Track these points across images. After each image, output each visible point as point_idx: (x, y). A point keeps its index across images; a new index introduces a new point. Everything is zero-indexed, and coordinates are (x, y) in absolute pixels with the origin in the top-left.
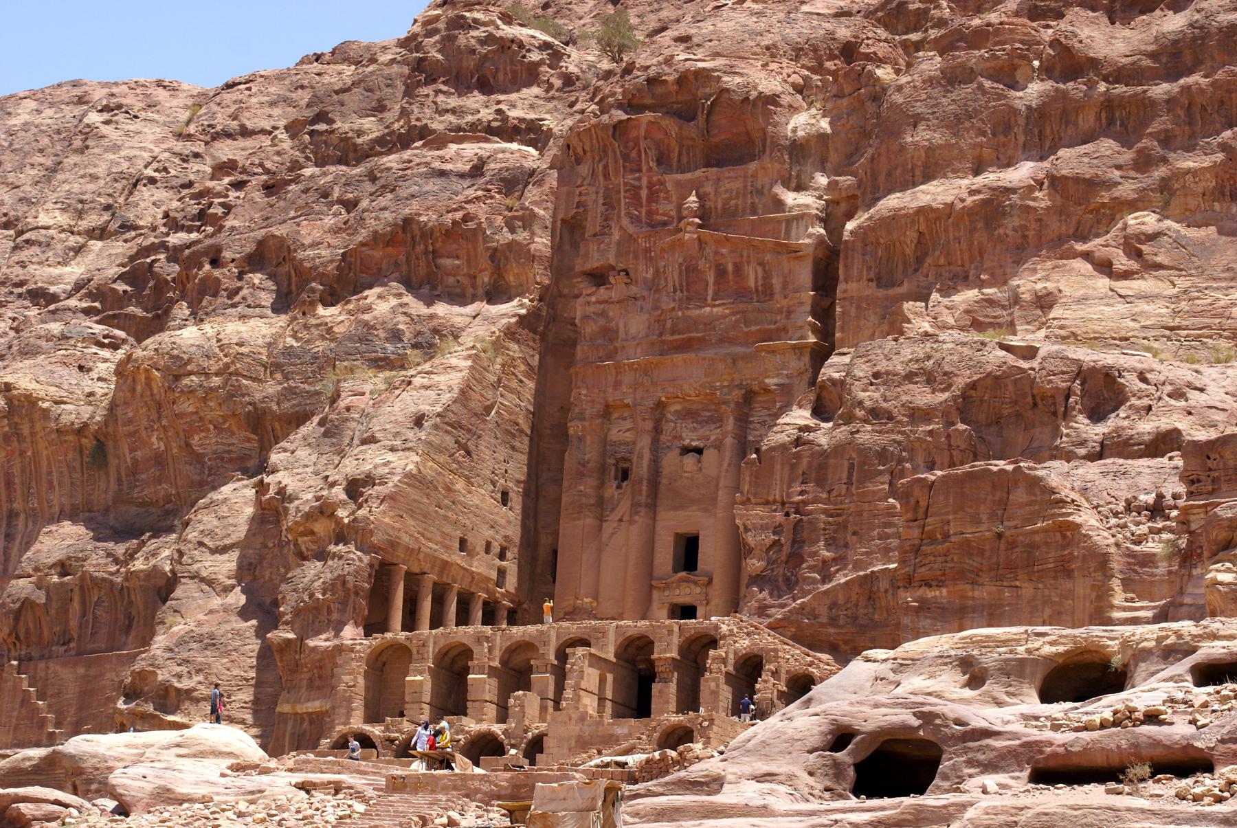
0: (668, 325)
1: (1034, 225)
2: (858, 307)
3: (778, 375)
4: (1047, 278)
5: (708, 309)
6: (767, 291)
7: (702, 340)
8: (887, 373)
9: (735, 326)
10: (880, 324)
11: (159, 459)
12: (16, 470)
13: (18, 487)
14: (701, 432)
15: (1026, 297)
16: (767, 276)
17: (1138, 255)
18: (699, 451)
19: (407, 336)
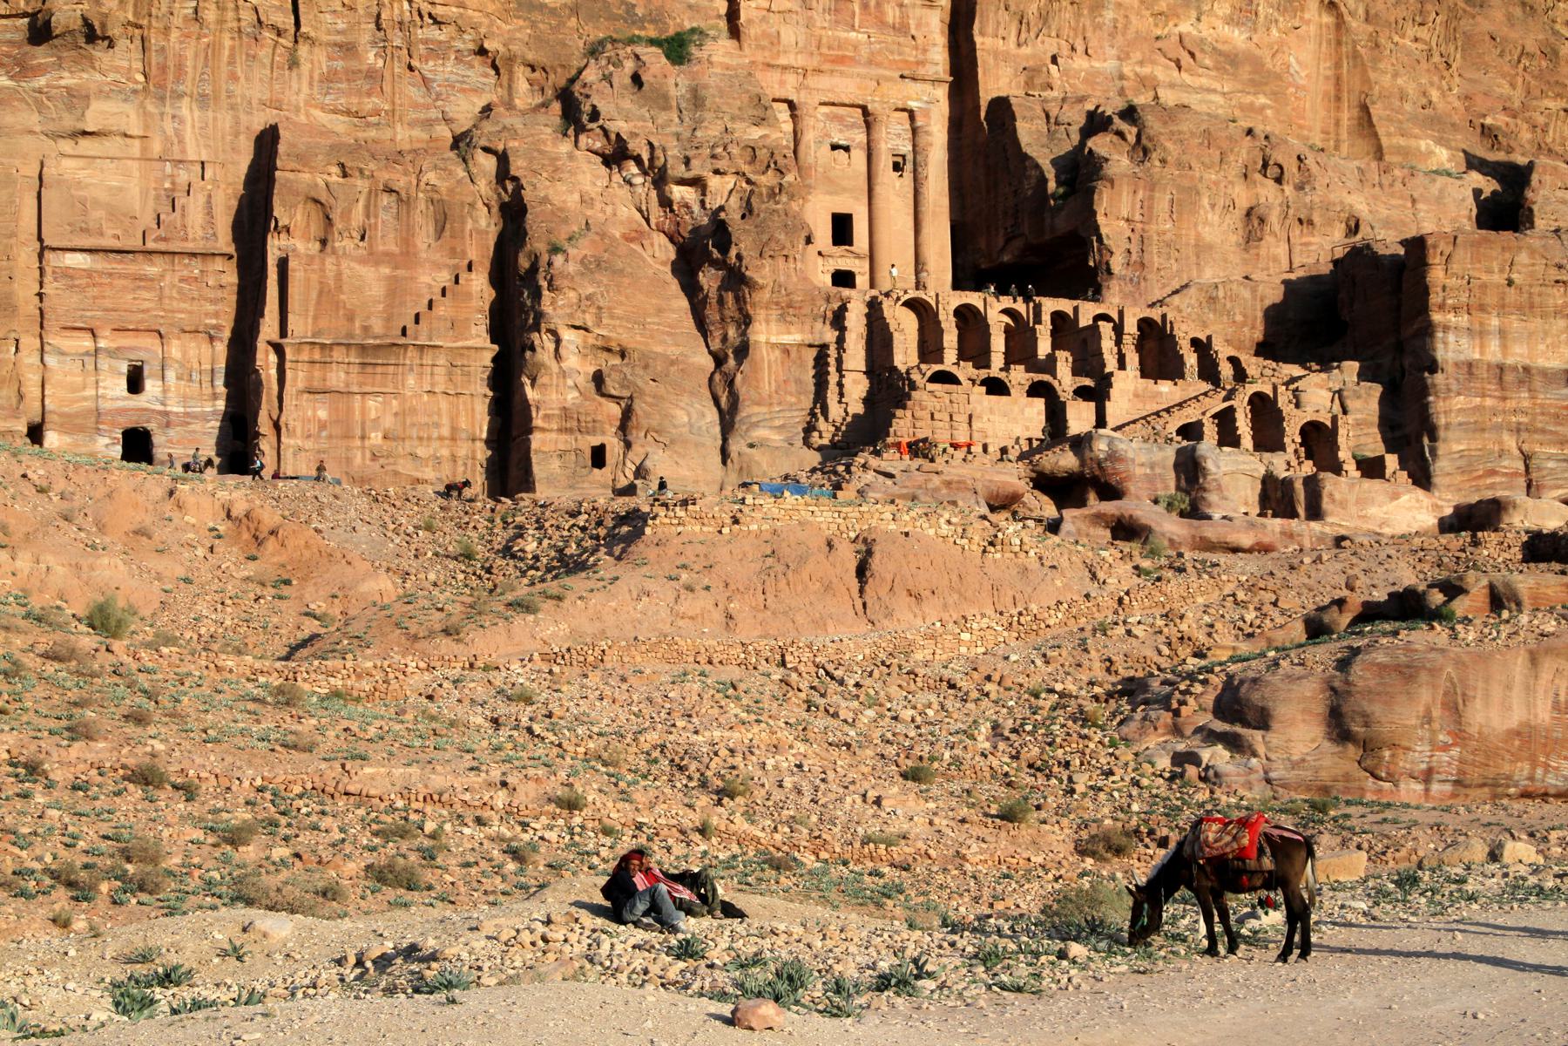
0: (824, 40)
1: (1121, 20)
2: (996, 59)
3: (917, 100)
4: (1141, 63)
5: (853, 35)
6: (902, 29)
7: (852, 59)
8: (1180, 132)
9: (880, 52)
10: (1016, 76)
11: (372, 75)
12: (190, 54)
13: (189, 70)
14: (848, 134)
15: (1131, 75)
16: (904, 16)
17: (1192, 55)
18: (847, 149)
19: (640, 11)
